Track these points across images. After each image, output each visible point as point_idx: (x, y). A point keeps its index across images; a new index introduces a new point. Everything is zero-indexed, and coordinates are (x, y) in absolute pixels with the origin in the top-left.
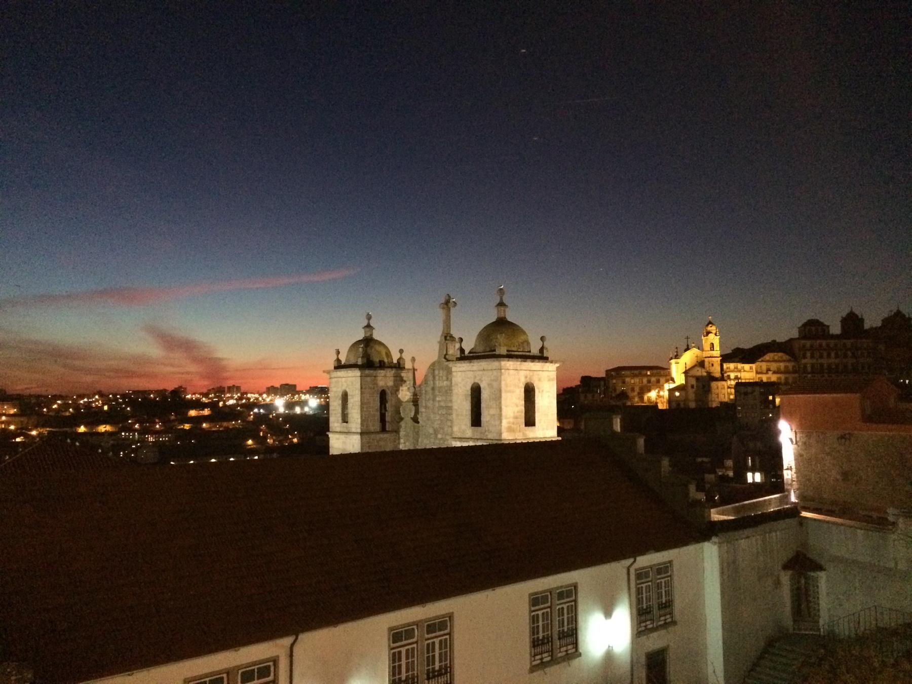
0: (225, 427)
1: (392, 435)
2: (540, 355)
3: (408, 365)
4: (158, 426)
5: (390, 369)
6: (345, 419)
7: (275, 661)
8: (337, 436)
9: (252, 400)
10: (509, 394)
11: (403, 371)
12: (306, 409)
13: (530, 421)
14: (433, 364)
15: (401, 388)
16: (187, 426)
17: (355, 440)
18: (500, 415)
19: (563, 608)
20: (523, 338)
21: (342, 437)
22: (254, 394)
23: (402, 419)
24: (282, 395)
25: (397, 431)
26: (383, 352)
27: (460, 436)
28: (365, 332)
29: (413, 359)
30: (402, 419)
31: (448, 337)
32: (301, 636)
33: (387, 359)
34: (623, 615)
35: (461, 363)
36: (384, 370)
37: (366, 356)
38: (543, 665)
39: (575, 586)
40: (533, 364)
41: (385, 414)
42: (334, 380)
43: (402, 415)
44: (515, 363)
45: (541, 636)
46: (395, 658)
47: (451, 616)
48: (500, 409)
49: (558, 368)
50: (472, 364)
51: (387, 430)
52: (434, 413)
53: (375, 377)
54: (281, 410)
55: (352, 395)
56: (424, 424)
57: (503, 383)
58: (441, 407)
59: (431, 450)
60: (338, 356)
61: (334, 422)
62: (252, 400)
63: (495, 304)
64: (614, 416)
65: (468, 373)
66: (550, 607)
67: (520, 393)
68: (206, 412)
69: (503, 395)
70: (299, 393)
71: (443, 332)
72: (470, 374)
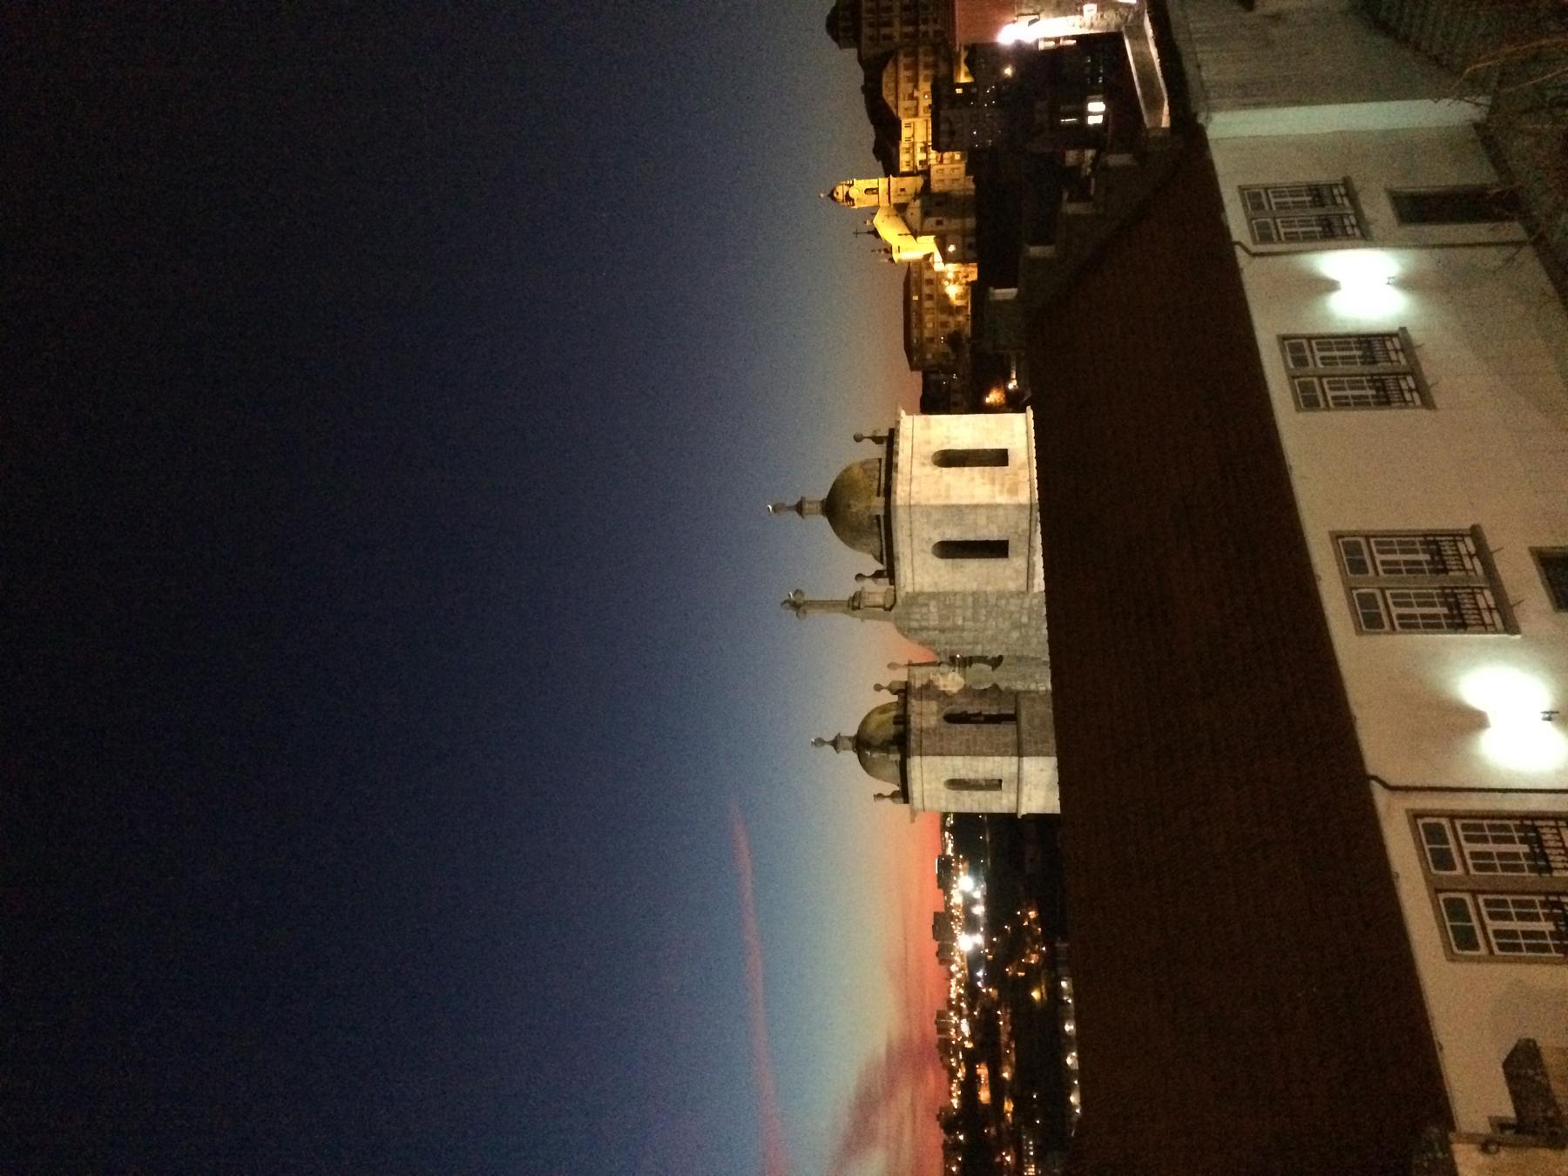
0: (1010, 1039)
1: (1022, 704)
2: (885, 445)
3: (901, 676)
4: (1008, 1159)
5: (909, 706)
6: (995, 785)
7: (1415, 816)
8: (1024, 800)
9: (962, 991)
10: (952, 493)
11: (913, 684)
12: (978, 895)
13: (999, 458)
14: (900, 629)
15: (942, 689)
16: (1009, 1106)
17: (1031, 766)
18: (989, 507)
19: (1322, 358)
20: (857, 472)
21: (1026, 790)
22: (951, 986)
23: (995, 687)
24: (953, 938)
25: (1016, 695)
26: (878, 718)
27: (1025, 578)
28: (845, 749)
29: (892, 666)
30: (995, 687)
31: (855, 604)
32: (1371, 771)
33: (890, 710)
34: (1331, 262)
35: (899, 575)
36: (910, 716)
37: (885, 747)
38: (1422, 390)
39: (1283, 339)
40: (900, 453)
41: (986, 716)
42: (927, 805)
43: (987, 686)
44: (899, 482)
45: (1371, 392)
46: (1408, 624)
47: (1336, 536)
48: (976, 506)
49: (908, 413)
50: (901, 556)
51: (1012, 712)
52: (985, 629)
53: (921, 731)
55: (954, 771)
56: (1004, 647)
57: (933, 502)
58: (975, 619)
59: (1053, 641)
60: (884, 797)
61: (1001, 804)
62: (962, 991)
63: (800, 518)
64: (991, 298)
65: (916, 564)
66: (1320, 377)
67: (951, 474)
68: (983, 1071)
69: (954, 501)
70: (948, 908)
71: (845, 612)
72: (918, 560)
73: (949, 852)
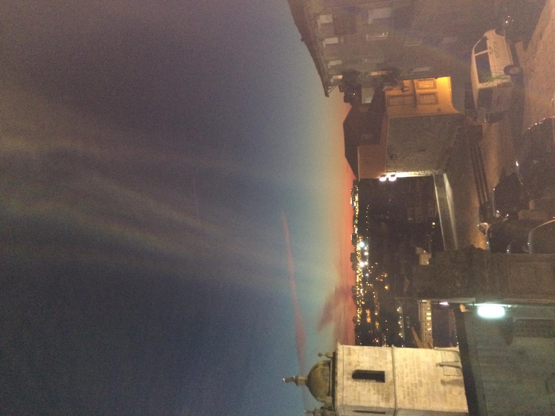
0: (378, 301)
4: (377, 341)
9: (361, 280)
10: (362, 398)
12: (366, 248)
16: (377, 324)
22: (357, 278)
24: (358, 262)
54: (366, 263)
62: (361, 280)
68: (368, 312)
70: (356, 252)
73: (356, 232)
